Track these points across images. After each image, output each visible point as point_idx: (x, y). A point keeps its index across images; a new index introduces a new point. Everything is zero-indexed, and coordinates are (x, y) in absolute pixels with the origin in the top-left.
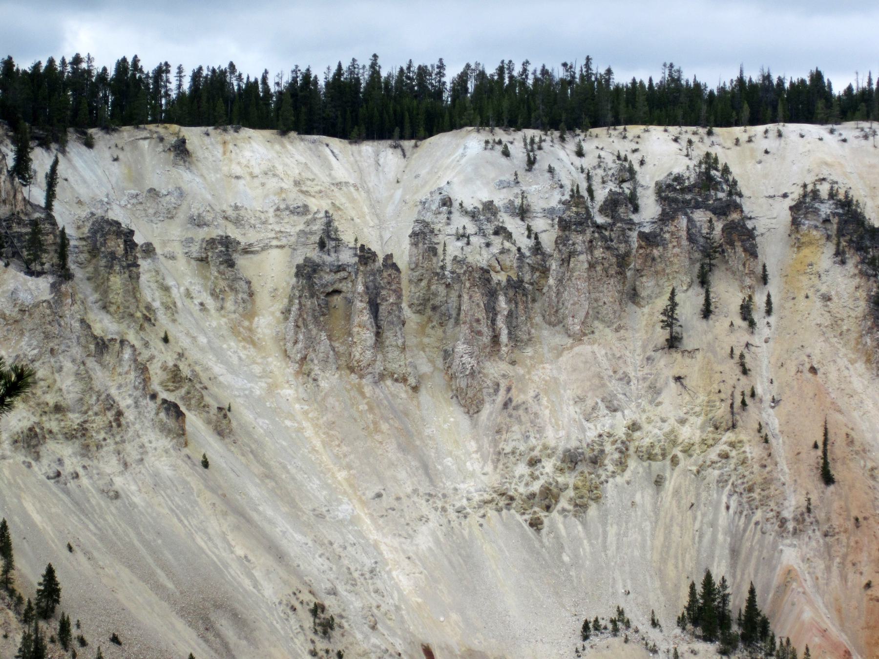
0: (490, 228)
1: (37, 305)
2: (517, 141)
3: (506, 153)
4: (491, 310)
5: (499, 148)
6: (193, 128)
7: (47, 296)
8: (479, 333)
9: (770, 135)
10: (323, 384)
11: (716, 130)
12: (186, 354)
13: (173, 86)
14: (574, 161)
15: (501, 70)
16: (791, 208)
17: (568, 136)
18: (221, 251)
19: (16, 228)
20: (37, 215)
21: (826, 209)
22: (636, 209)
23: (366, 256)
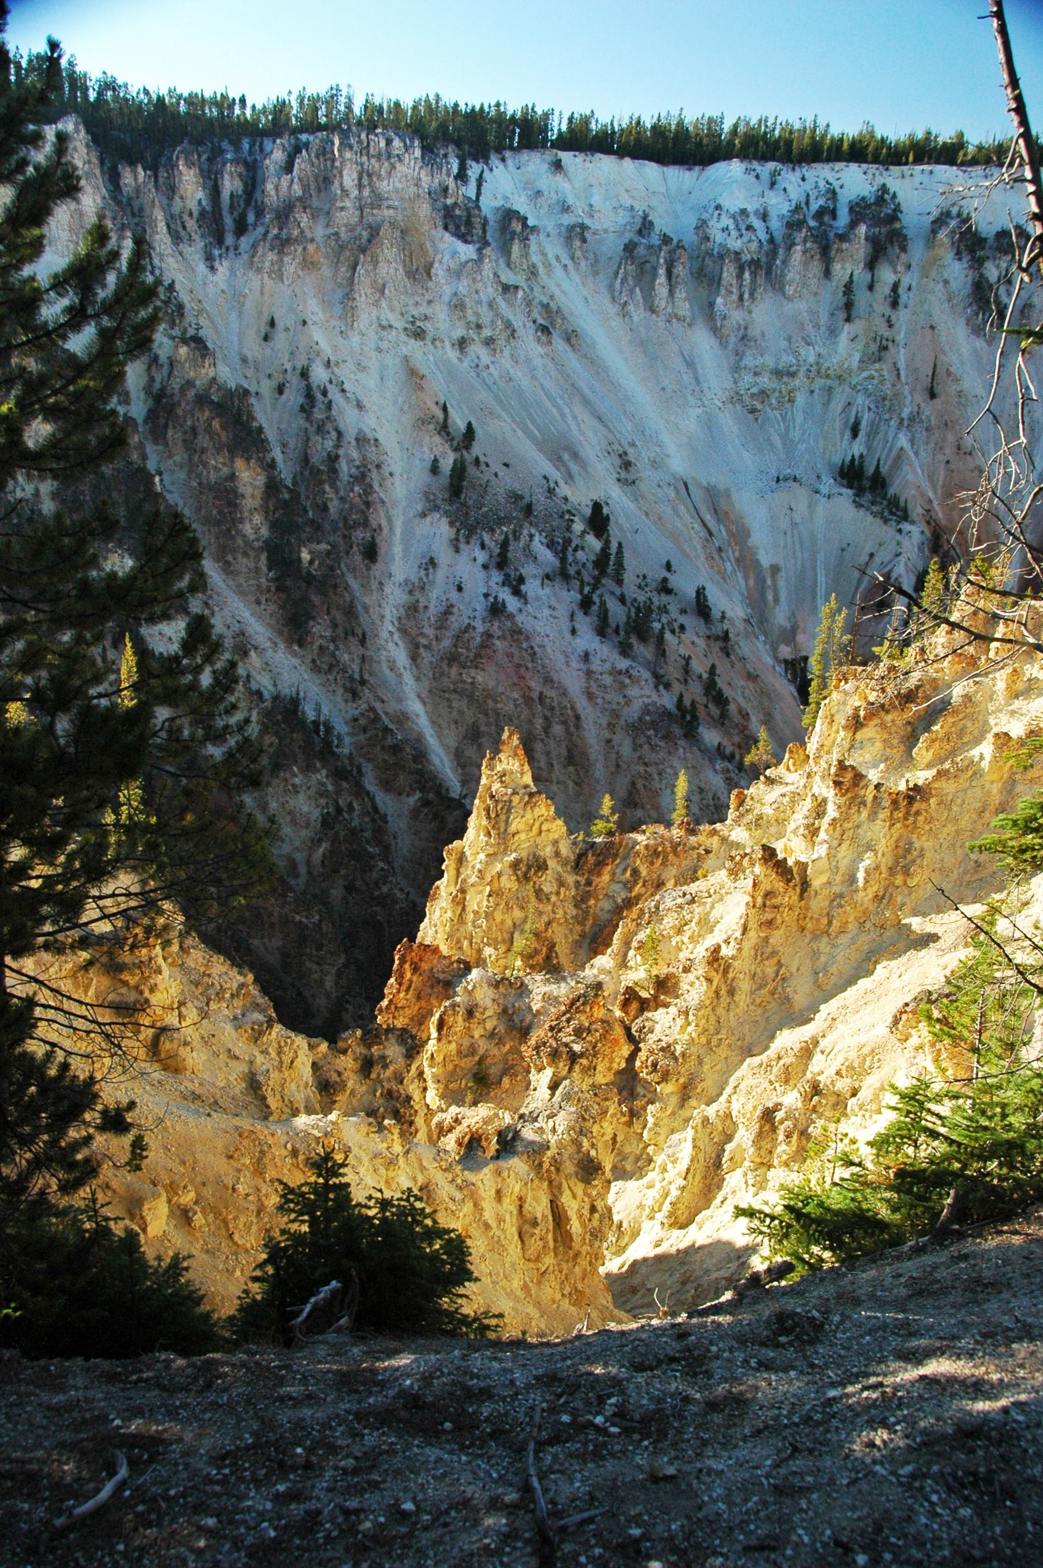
0: (743, 227)
3: (757, 177)
10: (636, 318)
13: (555, 124)
14: (800, 184)
19: (457, 212)
23: (666, 240)
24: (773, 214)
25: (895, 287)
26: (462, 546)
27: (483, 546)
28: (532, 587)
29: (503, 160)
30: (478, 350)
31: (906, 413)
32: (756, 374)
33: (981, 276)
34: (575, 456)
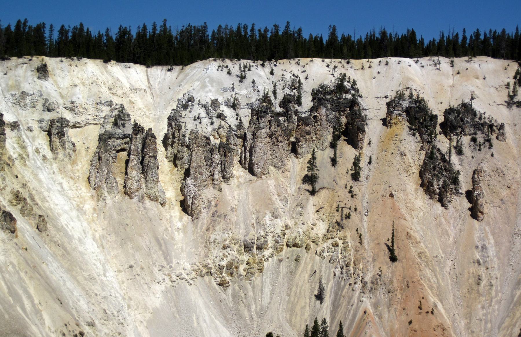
0: (214, 114)
2: (235, 67)
3: (229, 73)
4: (209, 161)
5: (225, 70)
6: (54, 58)
8: (201, 174)
9: (381, 64)
10: (109, 201)
11: (352, 61)
12: (28, 184)
13: (47, 35)
14: (265, 78)
15: (239, 28)
16: (387, 104)
17: (267, 63)
18: (58, 126)
21: (405, 104)
22: (299, 104)
23: (137, 129)
24: (242, 102)
25: (356, 163)
31: (368, 279)
32: (224, 248)
33: (434, 147)
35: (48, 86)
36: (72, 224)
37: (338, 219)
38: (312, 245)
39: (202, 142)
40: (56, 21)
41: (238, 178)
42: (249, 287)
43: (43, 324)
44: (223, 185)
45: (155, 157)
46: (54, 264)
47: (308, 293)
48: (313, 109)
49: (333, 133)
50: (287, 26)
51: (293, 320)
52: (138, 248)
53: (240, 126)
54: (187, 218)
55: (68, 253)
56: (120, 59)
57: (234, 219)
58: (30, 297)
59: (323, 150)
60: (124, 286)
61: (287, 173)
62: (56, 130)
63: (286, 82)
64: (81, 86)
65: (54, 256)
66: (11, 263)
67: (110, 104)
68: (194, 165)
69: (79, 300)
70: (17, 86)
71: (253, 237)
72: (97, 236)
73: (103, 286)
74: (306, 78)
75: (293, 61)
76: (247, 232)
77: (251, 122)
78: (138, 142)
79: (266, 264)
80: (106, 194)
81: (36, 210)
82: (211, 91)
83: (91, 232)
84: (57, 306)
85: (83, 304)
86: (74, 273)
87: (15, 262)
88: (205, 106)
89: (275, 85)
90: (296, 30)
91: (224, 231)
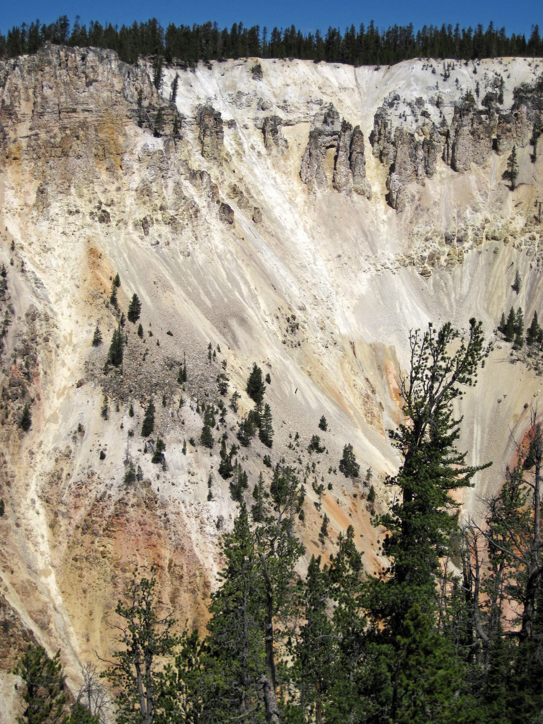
0: (418, 112)
1: (155, 153)
2: (439, 65)
3: (434, 72)
4: (413, 157)
5: (430, 70)
7: (162, 148)
8: (405, 169)
10: (319, 195)
13: (261, 37)
14: (468, 77)
15: (443, 28)
17: (470, 62)
20: (164, 105)
22: (501, 101)
23: (346, 126)
24: (446, 100)
26: (112, 413)
27: (132, 414)
28: (172, 454)
29: (210, 68)
30: (160, 230)
32: (427, 240)
34: (243, 321)
35: (262, 86)
36: (285, 216)
37: (536, 213)
38: (510, 238)
39: (407, 138)
40: (269, 24)
41: (440, 173)
42: (449, 276)
43: (259, 308)
44: (427, 181)
45: (362, 153)
46: (268, 253)
47: (505, 283)
48: (515, 107)
49: (534, 130)
50: (491, 26)
51: (490, 309)
52: (346, 239)
53: (443, 123)
54: (391, 211)
55: (281, 243)
56: (330, 59)
57: (436, 212)
58: (246, 283)
59: (523, 147)
60: (333, 274)
61: (487, 169)
62: (270, 128)
63: (488, 81)
64: (293, 85)
65: (268, 245)
66: (230, 252)
67: (320, 102)
68: (399, 160)
69: (291, 287)
70: (234, 86)
71: (453, 230)
72: (308, 227)
73: (314, 274)
74: (508, 77)
75: (496, 60)
76: (449, 225)
77: (454, 119)
78: (346, 139)
79: (465, 255)
80: (316, 188)
81: (252, 203)
82: (416, 90)
83: (302, 224)
84: (271, 292)
85: (295, 290)
86: (287, 261)
87: (233, 251)
88: (410, 104)
89: (478, 84)
90: (499, 29)
91: (427, 224)
